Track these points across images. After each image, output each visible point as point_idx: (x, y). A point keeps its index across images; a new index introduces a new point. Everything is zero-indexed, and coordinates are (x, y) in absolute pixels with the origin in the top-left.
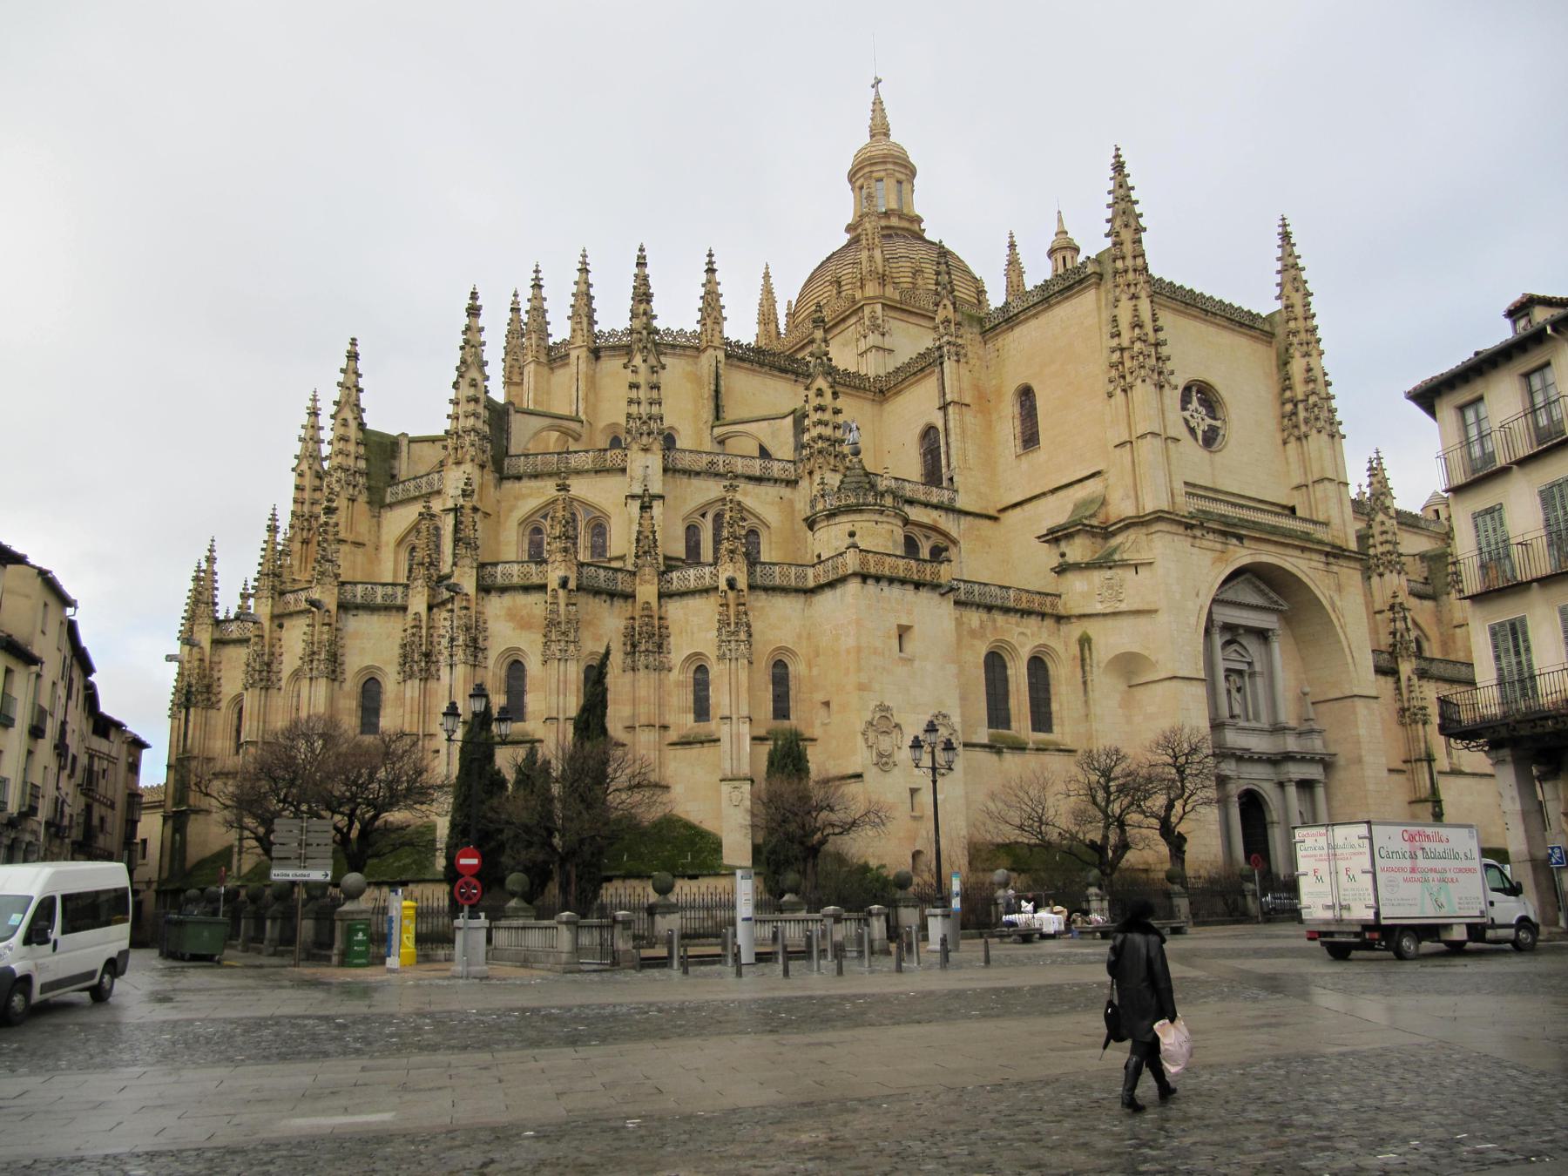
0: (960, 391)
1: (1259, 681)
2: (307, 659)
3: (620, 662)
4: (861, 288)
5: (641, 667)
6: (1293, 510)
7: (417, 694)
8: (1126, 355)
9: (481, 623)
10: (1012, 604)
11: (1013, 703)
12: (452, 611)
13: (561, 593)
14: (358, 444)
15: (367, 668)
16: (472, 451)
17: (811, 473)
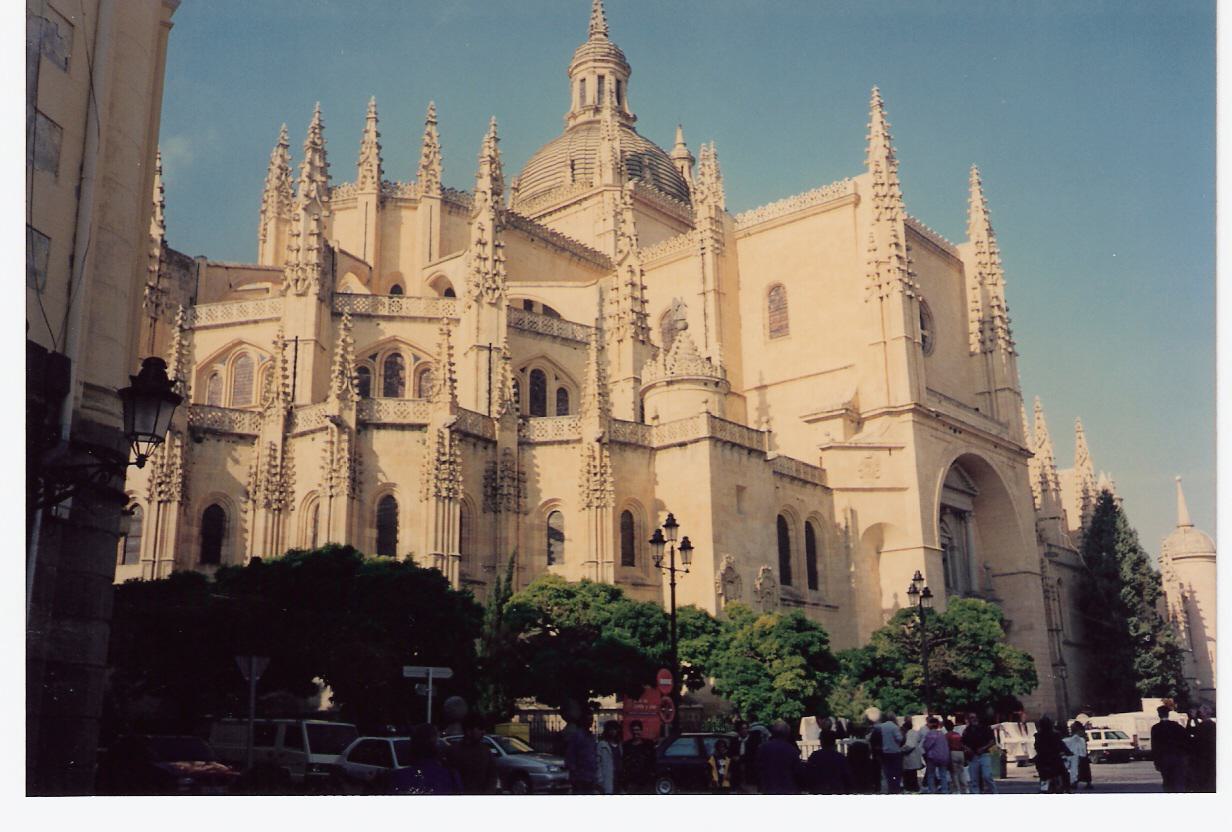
0: (718, 279)
1: (957, 554)
2: (155, 482)
3: (481, 503)
4: (601, 175)
5: (502, 509)
6: (977, 410)
7: (270, 525)
8: (883, 269)
9: (357, 457)
10: (795, 475)
11: (793, 561)
12: (332, 443)
13: (447, 432)
14: (161, 262)
15: (212, 494)
16: (314, 289)
17: (620, 341)
